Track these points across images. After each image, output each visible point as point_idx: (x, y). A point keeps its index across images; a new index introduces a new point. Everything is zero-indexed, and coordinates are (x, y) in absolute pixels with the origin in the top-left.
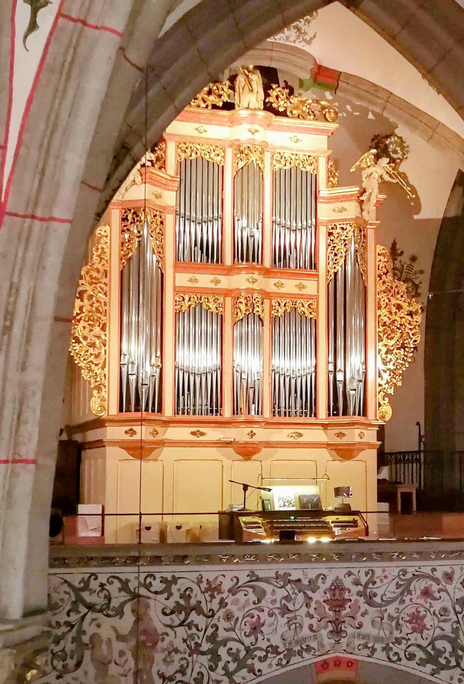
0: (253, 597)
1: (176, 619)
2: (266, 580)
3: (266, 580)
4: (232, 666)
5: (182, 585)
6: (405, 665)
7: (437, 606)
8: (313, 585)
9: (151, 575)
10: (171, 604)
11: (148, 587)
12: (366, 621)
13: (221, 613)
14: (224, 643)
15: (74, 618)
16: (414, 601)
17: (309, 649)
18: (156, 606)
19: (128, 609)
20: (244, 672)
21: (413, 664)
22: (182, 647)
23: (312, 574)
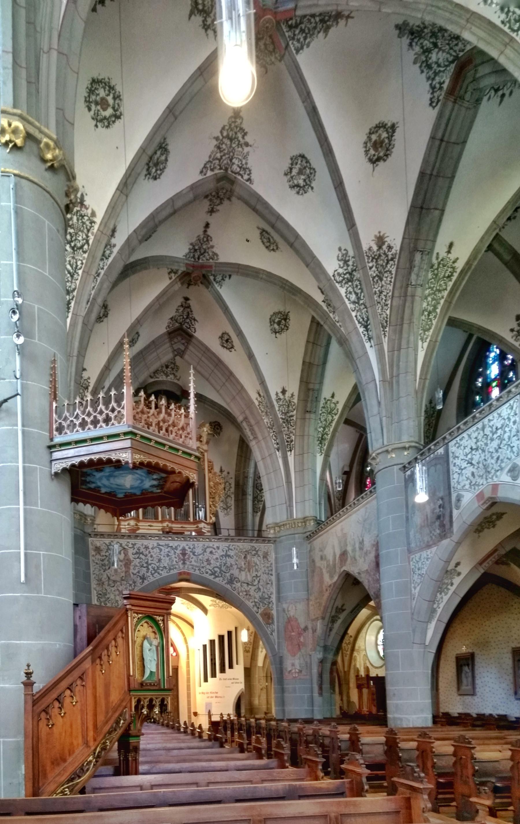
0: (158, 551)
1: (136, 556)
2: (162, 546)
3: (162, 546)
4: (153, 572)
5: (137, 546)
6: (205, 575)
7: (215, 557)
8: (176, 548)
9: (128, 542)
10: (134, 551)
11: (127, 546)
12: (193, 560)
13: (149, 555)
14: (150, 564)
15: (107, 554)
16: (207, 555)
17: (176, 568)
18: (131, 551)
19: (122, 552)
20: (156, 574)
21: (207, 575)
22: (138, 565)
23: (176, 545)
